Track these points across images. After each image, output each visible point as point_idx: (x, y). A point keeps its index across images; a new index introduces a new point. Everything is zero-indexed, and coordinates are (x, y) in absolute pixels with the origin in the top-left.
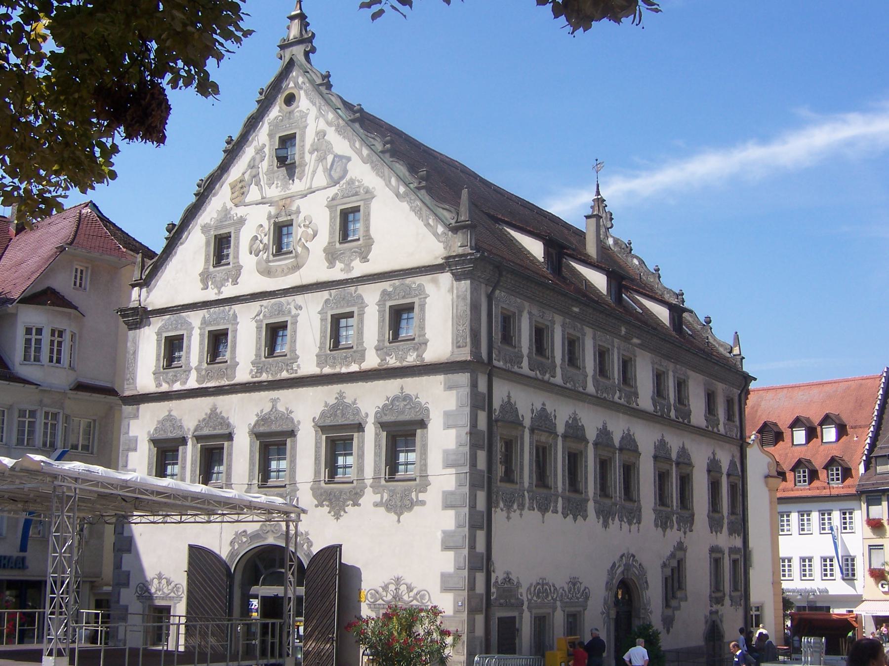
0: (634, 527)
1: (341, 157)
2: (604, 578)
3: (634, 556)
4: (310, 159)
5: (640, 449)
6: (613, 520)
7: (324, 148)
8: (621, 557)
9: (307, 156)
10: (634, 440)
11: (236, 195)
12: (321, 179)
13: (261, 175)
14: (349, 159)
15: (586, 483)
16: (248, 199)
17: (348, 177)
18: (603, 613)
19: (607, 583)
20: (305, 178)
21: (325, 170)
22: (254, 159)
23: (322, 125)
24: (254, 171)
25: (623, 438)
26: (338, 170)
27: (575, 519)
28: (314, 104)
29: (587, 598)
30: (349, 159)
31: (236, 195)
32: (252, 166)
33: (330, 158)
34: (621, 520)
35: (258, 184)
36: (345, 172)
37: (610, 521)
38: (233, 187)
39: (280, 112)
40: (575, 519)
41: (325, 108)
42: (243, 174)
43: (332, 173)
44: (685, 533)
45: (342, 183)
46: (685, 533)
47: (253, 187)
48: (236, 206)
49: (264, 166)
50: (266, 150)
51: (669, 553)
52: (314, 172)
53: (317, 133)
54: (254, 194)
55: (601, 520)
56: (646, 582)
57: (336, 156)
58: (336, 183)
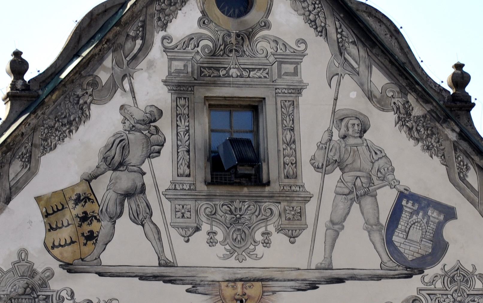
1: (423, 203)
4: (322, 189)
7: (364, 160)
9: (309, 178)
11: (65, 234)
12: (359, 249)
13: (151, 195)
14: (450, 213)
16: (110, 257)
17: (449, 260)
20: (305, 237)
21: (371, 227)
22: (121, 144)
23: (351, 97)
24: (125, 180)
26: (415, 234)
28: (323, 32)
30: (450, 213)
31: (65, 234)
32: (115, 159)
33: (386, 198)
35: (142, 218)
36: (440, 247)
38: (51, 210)
39: (204, 21)
41: (355, 52)
42: (89, 179)
43: (397, 238)
45: (430, 272)
47: (124, 223)
48: (69, 268)
49: (162, 170)
50: (165, 125)
52: (336, 226)
53: (339, 119)
54: (127, 243)
57: (404, 195)
58: (412, 270)
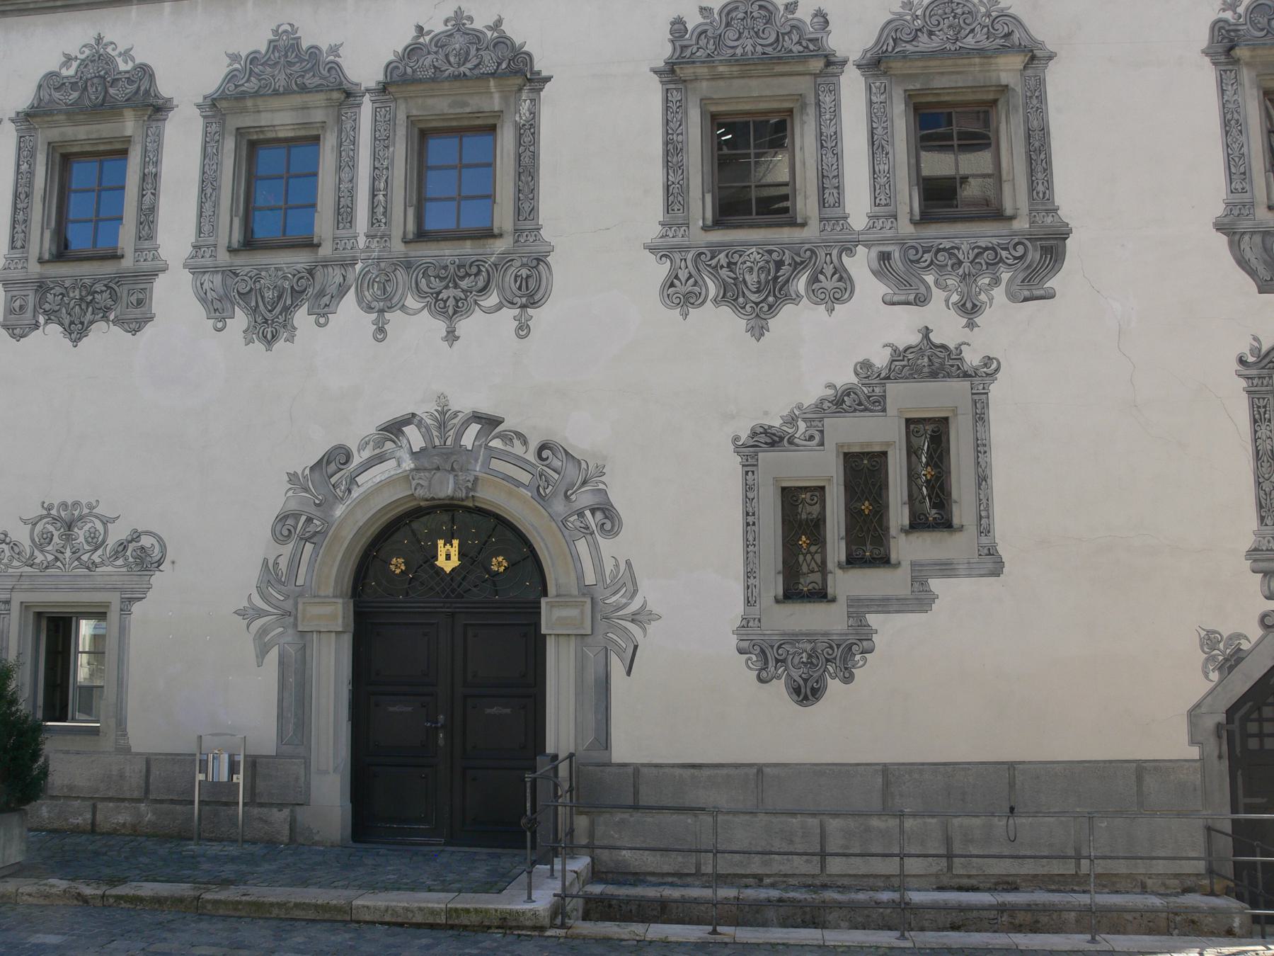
0: (488, 325)
2: (275, 497)
3: (489, 423)
5: (541, 65)
6: (323, 311)
8: (394, 429)
10: (502, 41)
15: (148, 216)
18: (249, 614)
19: (283, 518)
25: (412, 51)
27: (76, 331)
29: (144, 558)
34: (381, 304)
37: (302, 317)
40: (76, 331)
44: (970, 309)
46: (970, 309)
51: (813, 392)
55: (240, 320)
56: (606, 510)
